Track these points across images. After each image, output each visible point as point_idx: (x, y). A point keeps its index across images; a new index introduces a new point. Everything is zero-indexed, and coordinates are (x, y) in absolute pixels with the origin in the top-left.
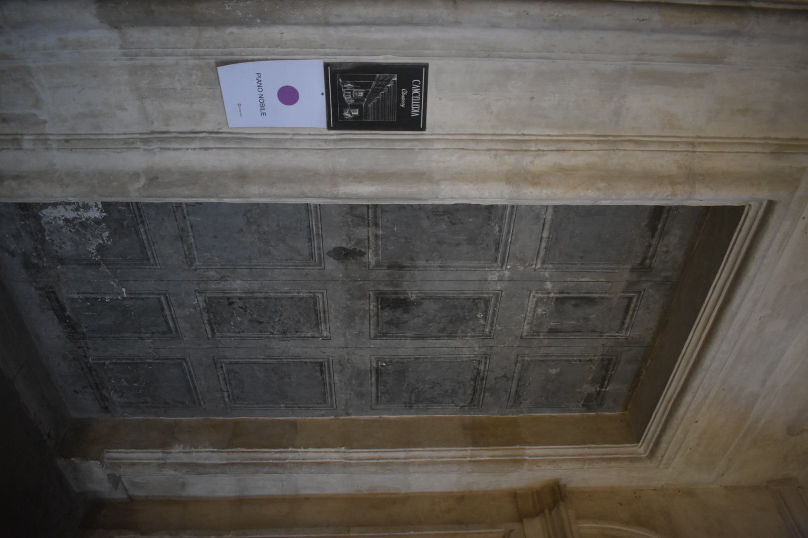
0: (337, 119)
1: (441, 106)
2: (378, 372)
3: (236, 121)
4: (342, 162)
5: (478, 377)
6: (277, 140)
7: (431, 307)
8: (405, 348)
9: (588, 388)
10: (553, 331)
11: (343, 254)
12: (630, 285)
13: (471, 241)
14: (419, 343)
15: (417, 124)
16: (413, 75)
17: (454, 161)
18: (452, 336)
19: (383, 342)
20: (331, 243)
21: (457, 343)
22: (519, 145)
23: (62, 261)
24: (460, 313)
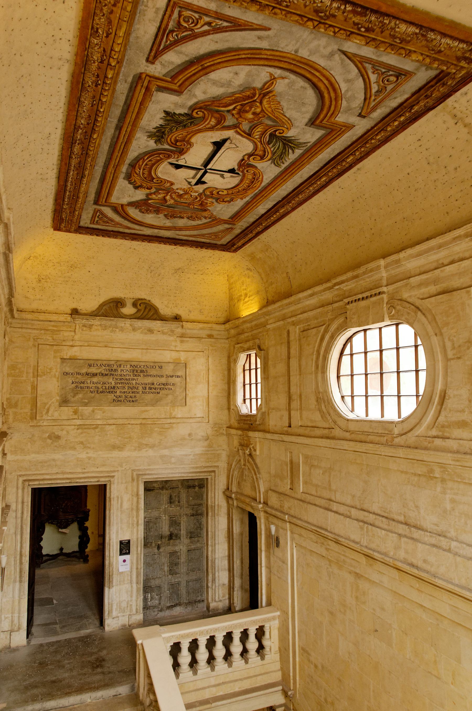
0: (129, 553)
1: (126, 537)
2: (191, 538)
3: (129, 569)
4: (135, 552)
5: (193, 515)
6: (132, 563)
7: (171, 529)
8: (183, 532)
9: (197, 488)
10: (179, 502)
11: (159, 548)
12: (167, 489)
13: (156, 524)
14: (182, 530)
15: (129, 541)
16: (121, 542)
17: (135, 534)
18: (180, 523)
19: (182, 538)
20: (156, 551)
21: (182, 522)
22: (133, 524)
23: (160, 604)
24: (174, 522)
